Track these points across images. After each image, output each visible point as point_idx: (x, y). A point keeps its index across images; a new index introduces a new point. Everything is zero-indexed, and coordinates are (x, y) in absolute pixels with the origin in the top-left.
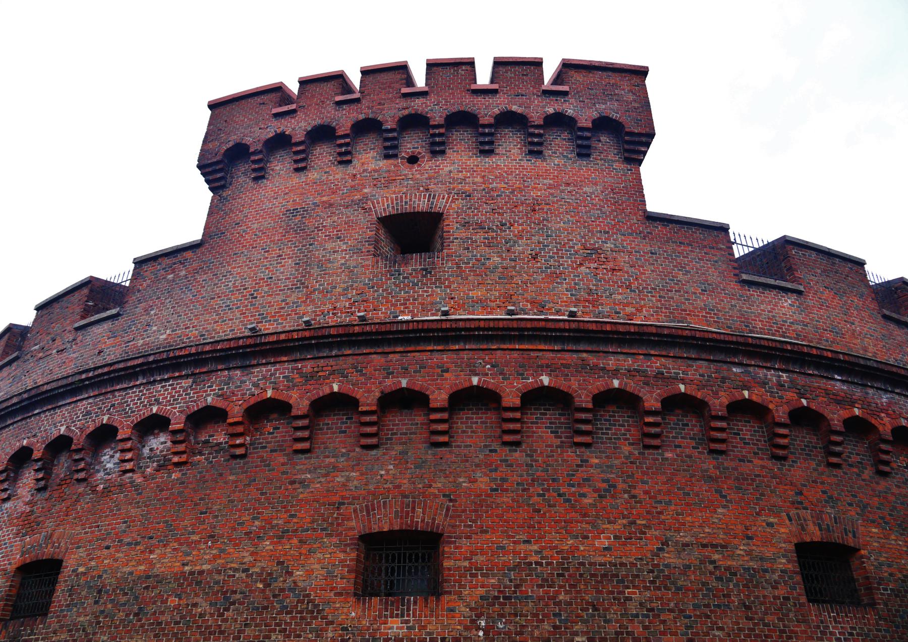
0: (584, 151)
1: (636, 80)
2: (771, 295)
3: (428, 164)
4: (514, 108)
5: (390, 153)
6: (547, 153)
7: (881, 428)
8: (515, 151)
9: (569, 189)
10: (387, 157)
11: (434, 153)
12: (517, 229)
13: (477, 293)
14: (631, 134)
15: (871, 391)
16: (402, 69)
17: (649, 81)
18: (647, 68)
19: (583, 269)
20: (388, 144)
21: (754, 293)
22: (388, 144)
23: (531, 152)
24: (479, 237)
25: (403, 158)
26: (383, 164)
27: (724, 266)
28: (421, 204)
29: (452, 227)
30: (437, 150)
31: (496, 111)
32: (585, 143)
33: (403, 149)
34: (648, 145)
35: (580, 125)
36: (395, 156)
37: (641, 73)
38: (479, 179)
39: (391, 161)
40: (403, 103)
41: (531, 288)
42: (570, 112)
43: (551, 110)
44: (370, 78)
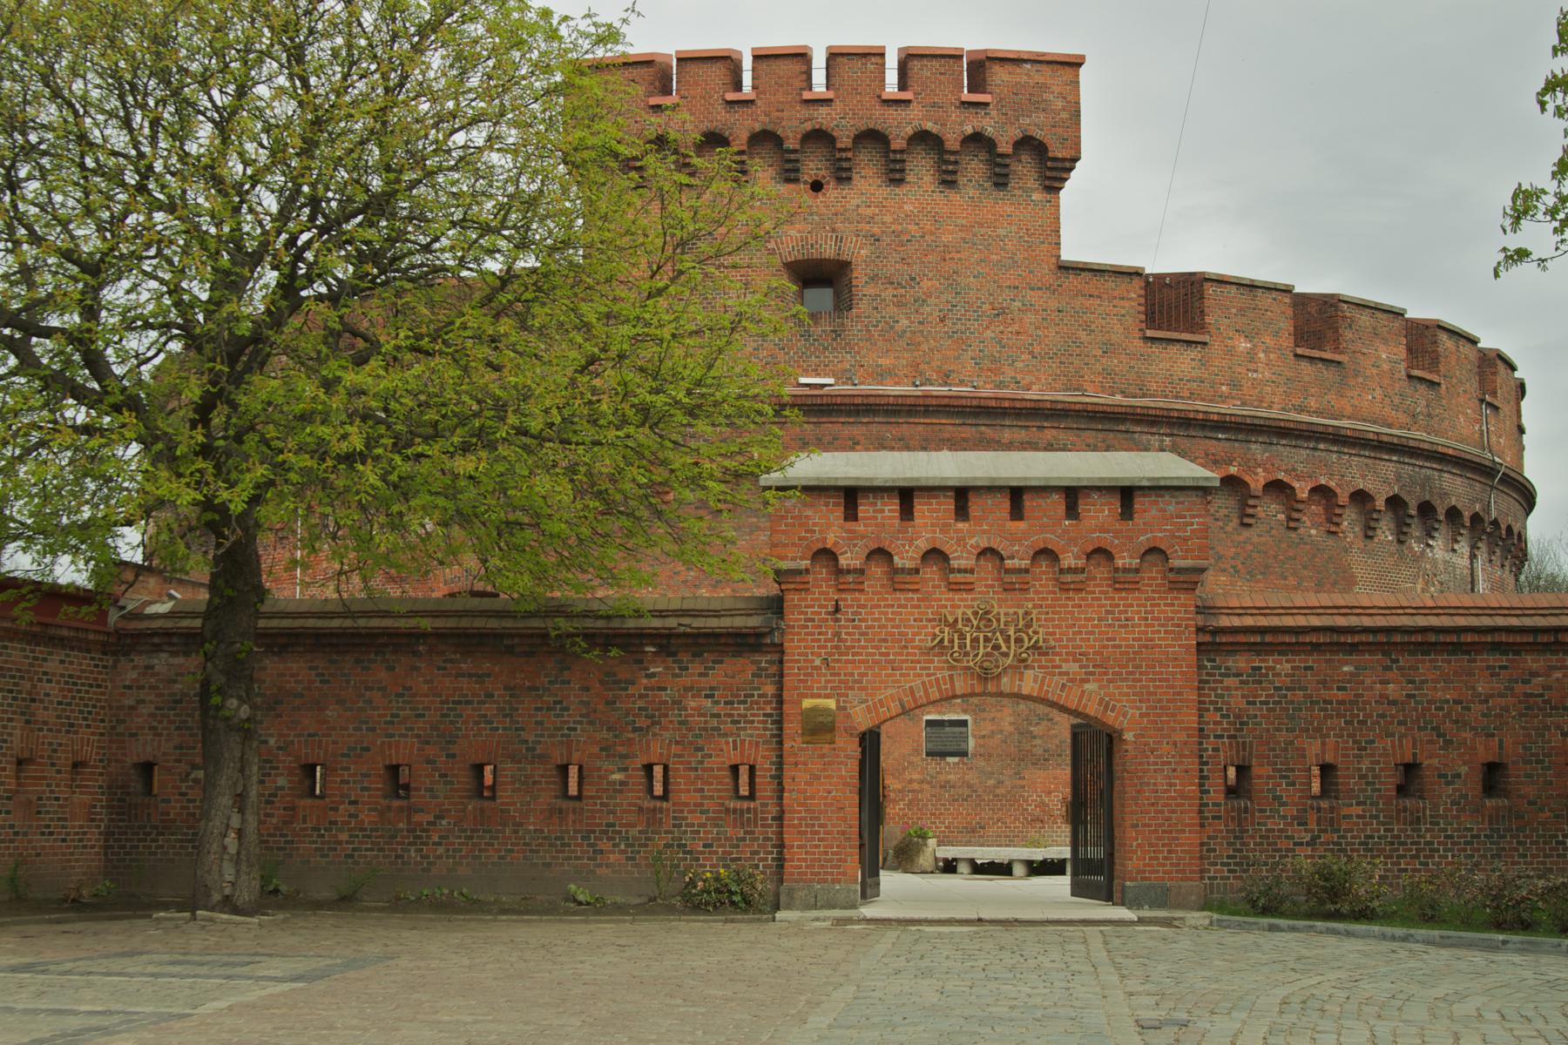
0: (1001, 181)
1: (1067, 73)
2: (1174, 349)
3: (832, 193)
4: (929, 126)
5: (790, 175)
6: (962, 180)
7: (1252, 486)
8: (928, 179)
9: (982, 231)
10: (788, 180)
11: (840, 180)
12: (926, 284)
13: (885, 362)
14: (1055, 159)
15: (1253, 446)
16: (801, 57)
17: (1082, 70)
18: (1083, 57)
19: (988, 333)
20: (789, 166)
21: (1155, 349)
22: (789, 166)
23: (944, 182)
24: (889, 293)
25: (805, 183)
26: (784, 189)
27: (1130, 320)
28: (828, 251)
29: (859, 276)
30: (843, 176)
31: (909, 130)
32: (1003, 171)
33: (804, 169)
34: (1071, 169)
35: (1000, 150)
36: (796, 180)
37: (1074, 64)
38: (888, 219)
39: (792, 186)
40: (805, 112)
41: (937, 356)
42: (990, 131)
43: (969, 130)
44: (764, 65)
